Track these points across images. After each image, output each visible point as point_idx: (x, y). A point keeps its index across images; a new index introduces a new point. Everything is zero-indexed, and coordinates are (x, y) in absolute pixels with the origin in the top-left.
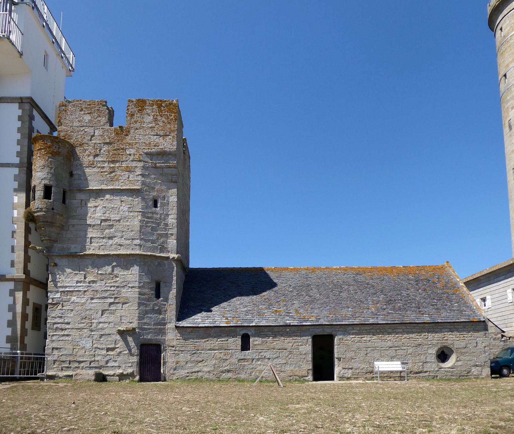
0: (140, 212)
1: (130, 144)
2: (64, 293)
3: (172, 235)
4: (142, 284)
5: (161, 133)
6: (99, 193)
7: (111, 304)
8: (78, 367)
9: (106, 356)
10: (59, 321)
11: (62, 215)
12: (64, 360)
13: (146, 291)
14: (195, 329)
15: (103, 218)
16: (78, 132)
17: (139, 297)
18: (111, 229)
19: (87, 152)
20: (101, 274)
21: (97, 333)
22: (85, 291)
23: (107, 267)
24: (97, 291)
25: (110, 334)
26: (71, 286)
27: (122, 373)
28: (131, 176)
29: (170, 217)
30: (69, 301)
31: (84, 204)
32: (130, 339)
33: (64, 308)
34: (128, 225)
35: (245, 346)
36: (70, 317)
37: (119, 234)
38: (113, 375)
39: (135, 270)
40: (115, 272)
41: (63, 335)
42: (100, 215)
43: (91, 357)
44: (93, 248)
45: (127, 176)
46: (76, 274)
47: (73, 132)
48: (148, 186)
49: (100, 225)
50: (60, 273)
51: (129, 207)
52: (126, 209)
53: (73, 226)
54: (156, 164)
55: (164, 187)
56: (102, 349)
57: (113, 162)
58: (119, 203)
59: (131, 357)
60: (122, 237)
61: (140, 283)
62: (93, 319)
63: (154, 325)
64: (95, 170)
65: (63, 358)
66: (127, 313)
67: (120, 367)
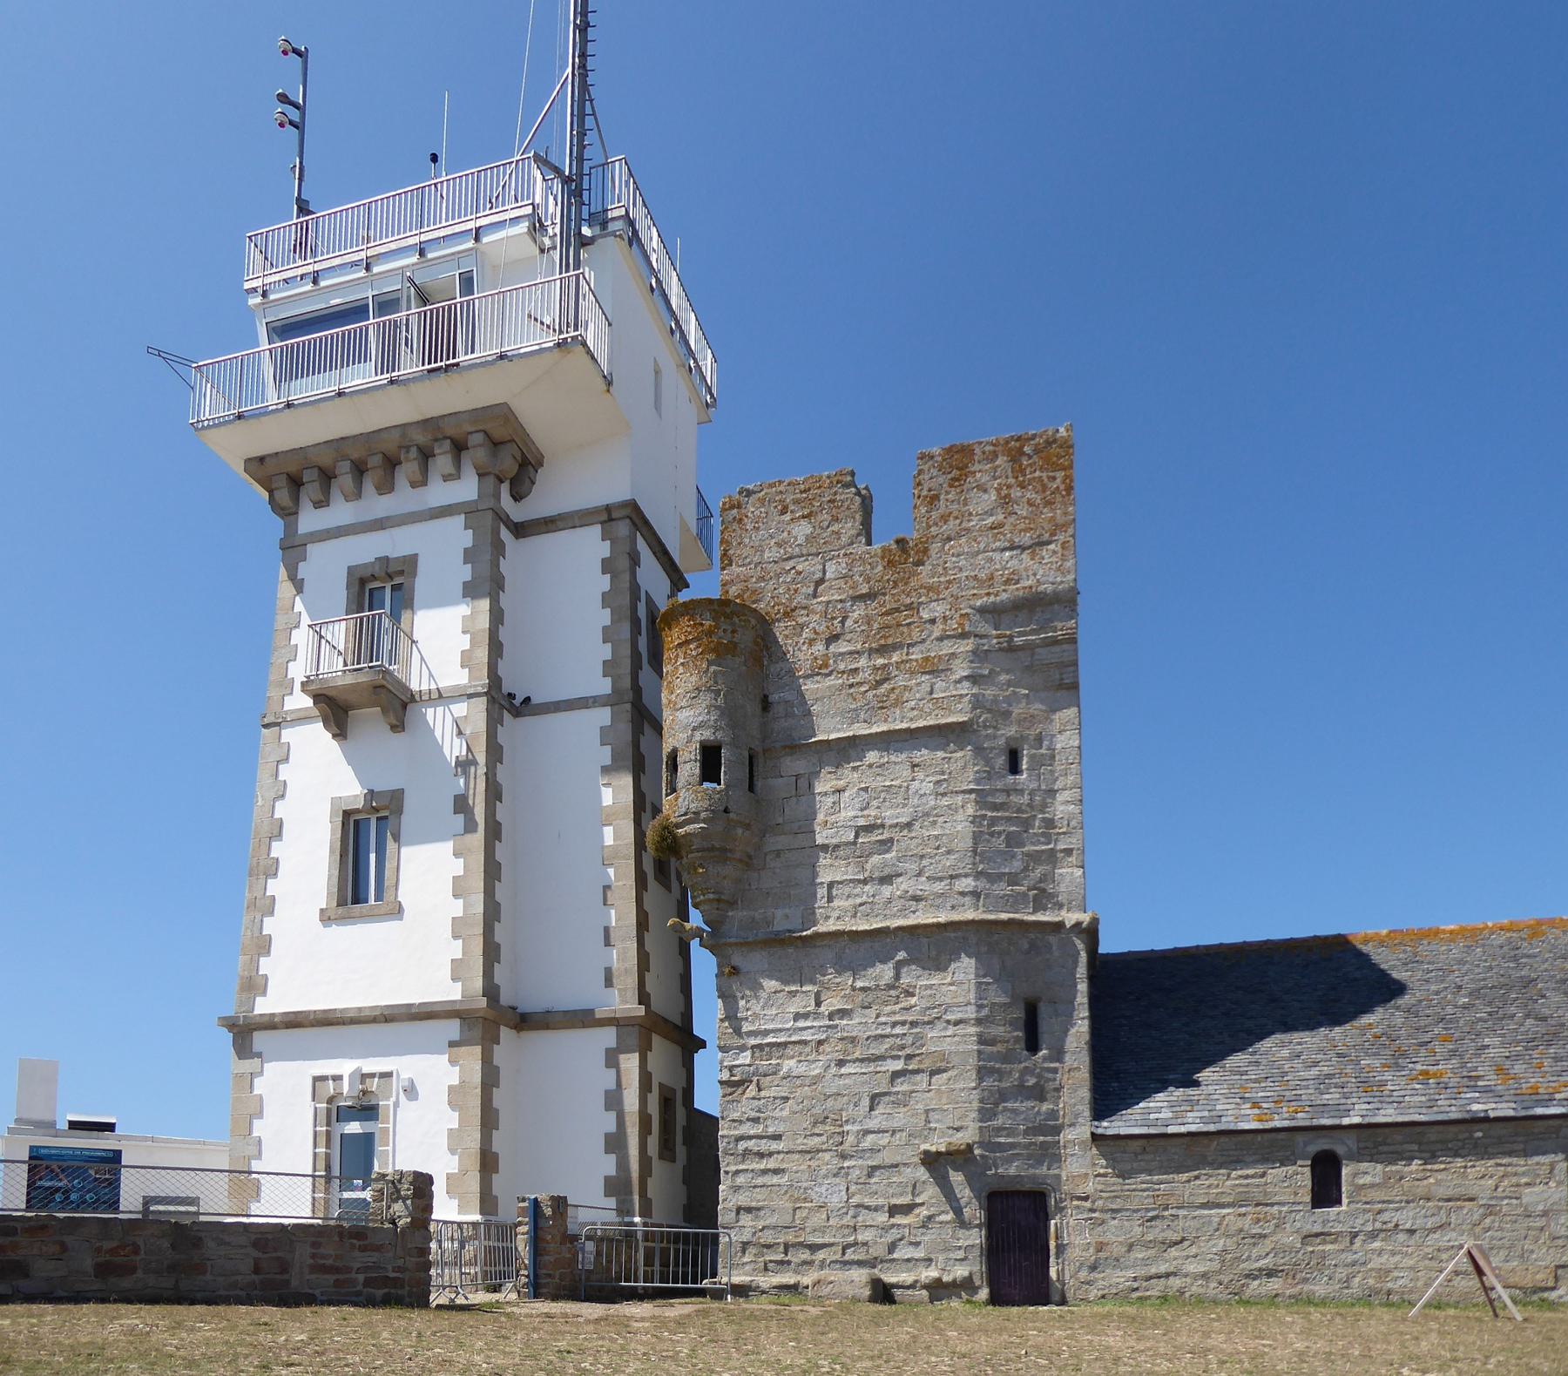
0: (971, 791)
1: (930, 589)
3: (1069, 852)
4: (985, 1012)
6: (847, 750)
7: (896, 1075)
8: (810, 1263)
9: (886, 1229)
10: (752, 1132)
11: (747, 827)
12: (770, 1240)
13: (999, 1031)
14: (1152, 1142)
15: (861, 822)
16: (778, 576)
17: (979, 1052)
19: (807, 633)
20: (863, 989)
21: (860, 1162)
22: (820, 1043)
23: (879, 967)
24: (853, 1040)
25: (896, 1166)
26: (780, 1030)
27: (939, 1280)
28: (939, 685)
29: (1060, 797)
30: (775, 1073)
31: (803, 787)
32: (956, 1177)
33: (763, 1094)
34: (936, 837)
35: (1325, 1191)
36: (781, 1119)
37: (913, 867)
38: (912, 1286)
39: (965, 968)
40: (905, 980)
41: (765, 1172)
43: (846, 1231)
44: (836, 914)
45: (926, 688)
46: (793, 994)
47: (762, 579)
48: (990, 711)
49: (855, 843)
51: (938, 782)
52: (927, 787)
53: (778, 853)
54: (1011, 637)
55: (1037, 707)
56: (876, 1209)
57: (883, 650)
58: (907, 773)
59: (961, 1233)
60: (919, 875)
61: (980, 1007)
63: (1026, 1133)
65: (768, 1237)
67: (930, 1260)
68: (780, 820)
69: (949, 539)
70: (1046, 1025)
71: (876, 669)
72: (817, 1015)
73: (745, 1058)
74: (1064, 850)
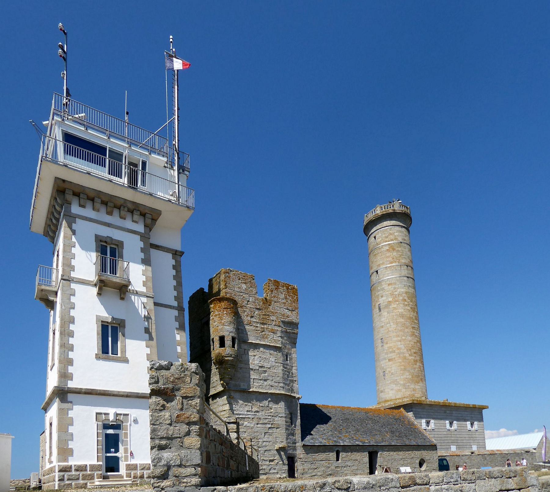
1: (272, 312)
5: (290, 308)
6: (256, 346)
7: (269, 428)
20: (262, 406)
23: (265, 401)
24: (260, 418)
29: (294, 368)
32: (282, 453)
37: (270, 378)
39: (282, 405)
47: (235, 295)
53: (241, 368)
57: (263, 324)
64: (251, 327)
70: (294, 419)
71: (262, 328)
72: (252, 411)
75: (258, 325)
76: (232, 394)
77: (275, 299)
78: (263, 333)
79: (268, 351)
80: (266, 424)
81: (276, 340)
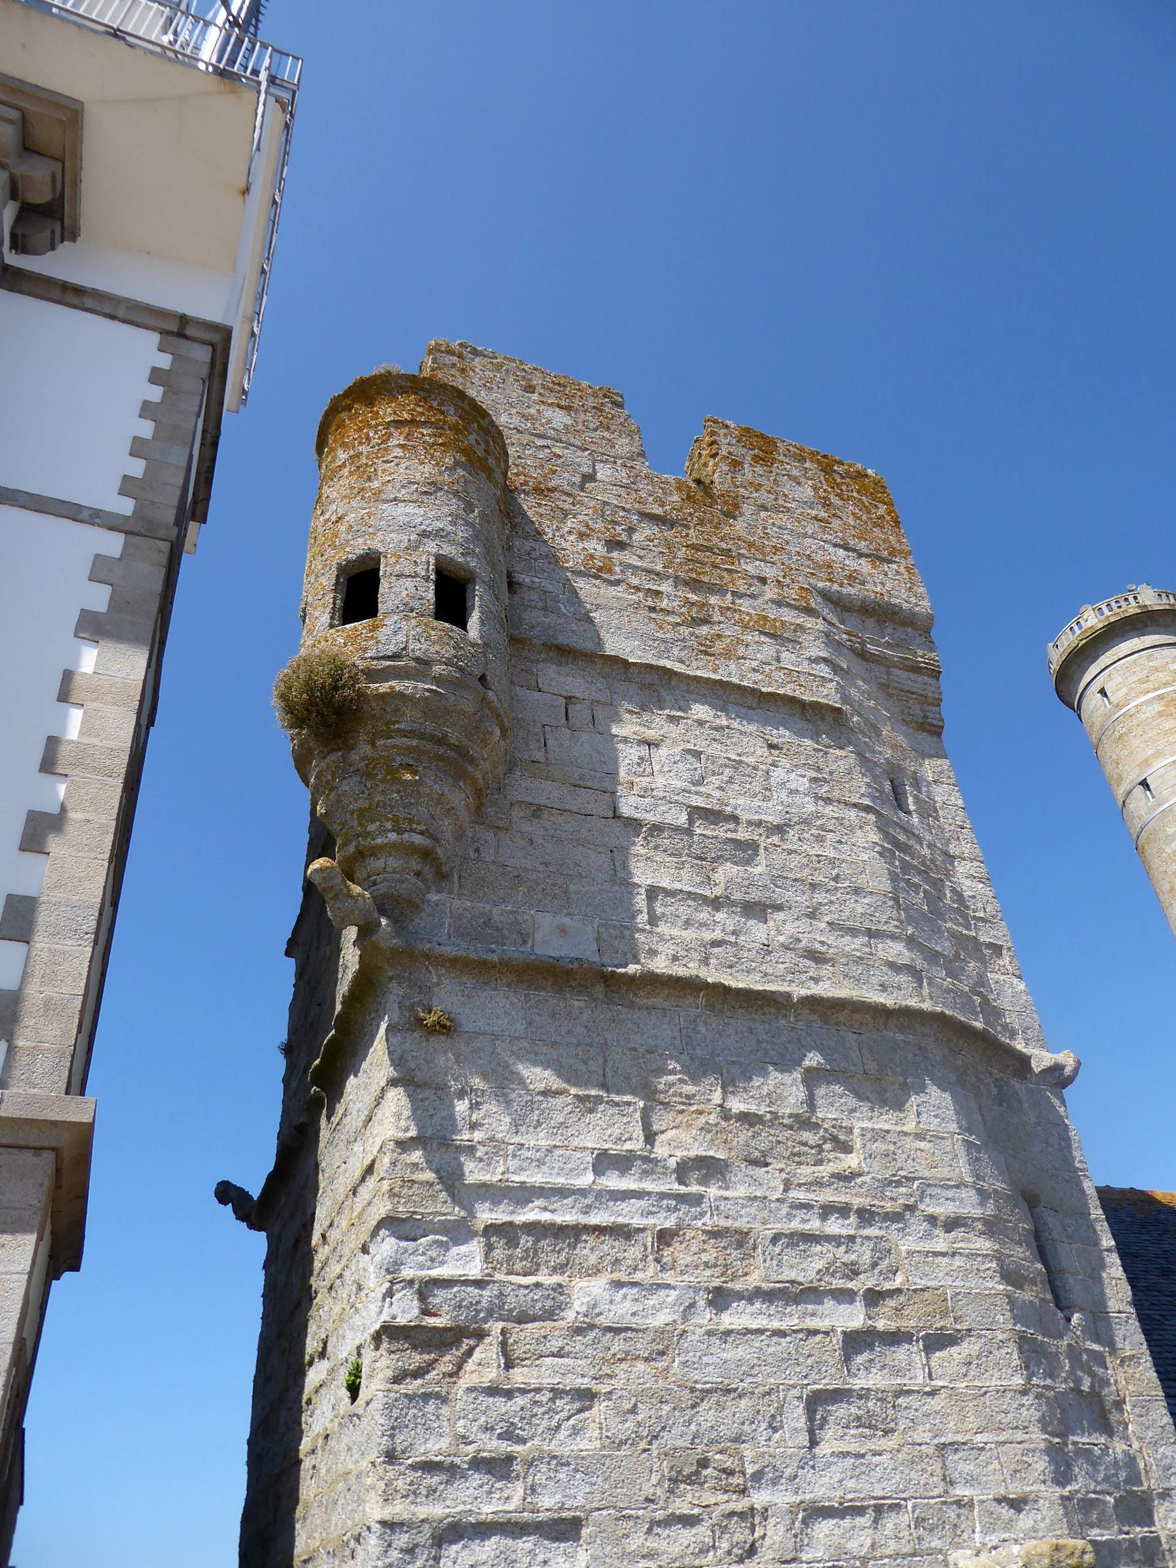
1: (751, 545)
2: (512, 1243)
18: (748, 862)
20: (747, 1119)
22: (664, 1237)
24: (741, 1238)
26: (562, 1192)
30: (550, 1315)
36: (579, 1465)
37: (800, 899)
42: (678, 784)
46: (587, 1105)
49: (689, 832)
50: (477, 1082)
57: (695, 584)
60: (813, 915)
62: (758, 1476)
64: (613, 591)
66: (972, 1423)
68: (539, 756)
69: (764, 508)
72: (651, 1165)
73: (466, 1260)
74: (990, 945)
75: (665, 587)
76: (447, 996)
77: (763, 496)
78: (704, 630)
79: (751, 728)
80: (808, 1294)
81: (804, 666)
